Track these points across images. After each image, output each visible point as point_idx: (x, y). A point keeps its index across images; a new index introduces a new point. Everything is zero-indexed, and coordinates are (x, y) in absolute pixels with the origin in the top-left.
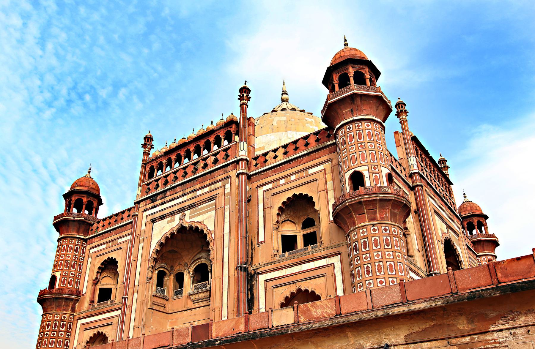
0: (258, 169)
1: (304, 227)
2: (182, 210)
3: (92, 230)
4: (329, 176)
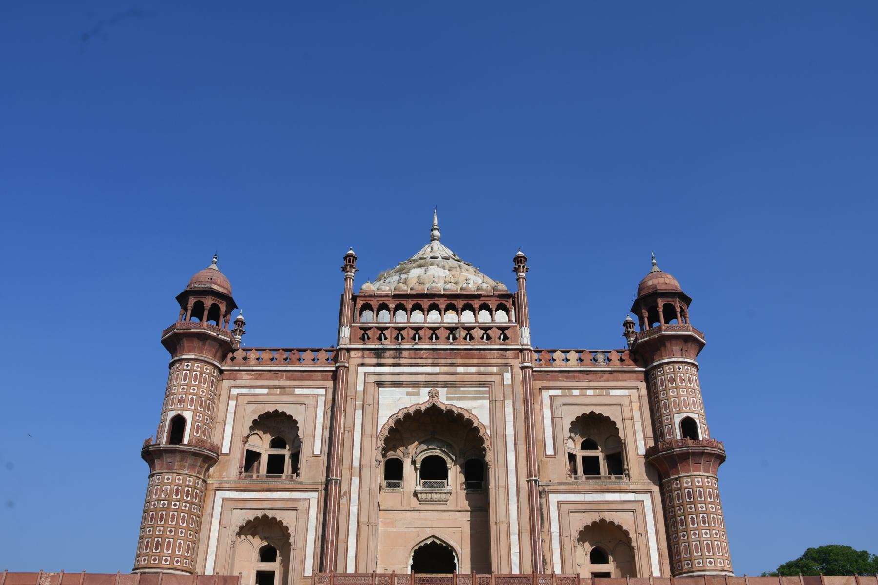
0: (541, 366)
1: (585, 446)
2: (435, 384)
3: (233, 359)
4: (636, 406)
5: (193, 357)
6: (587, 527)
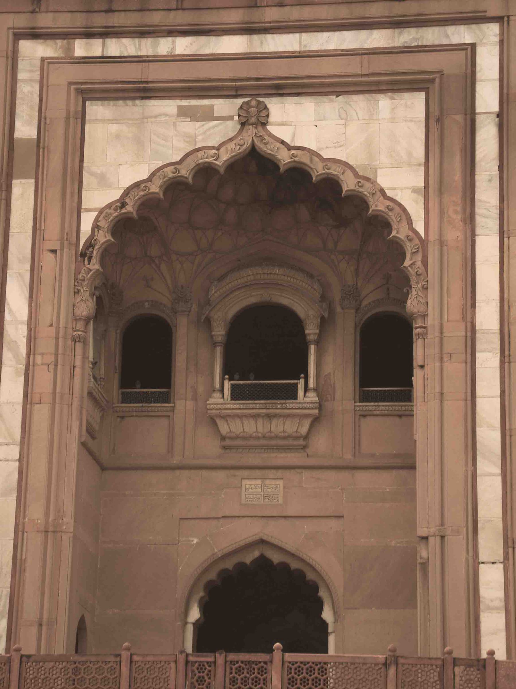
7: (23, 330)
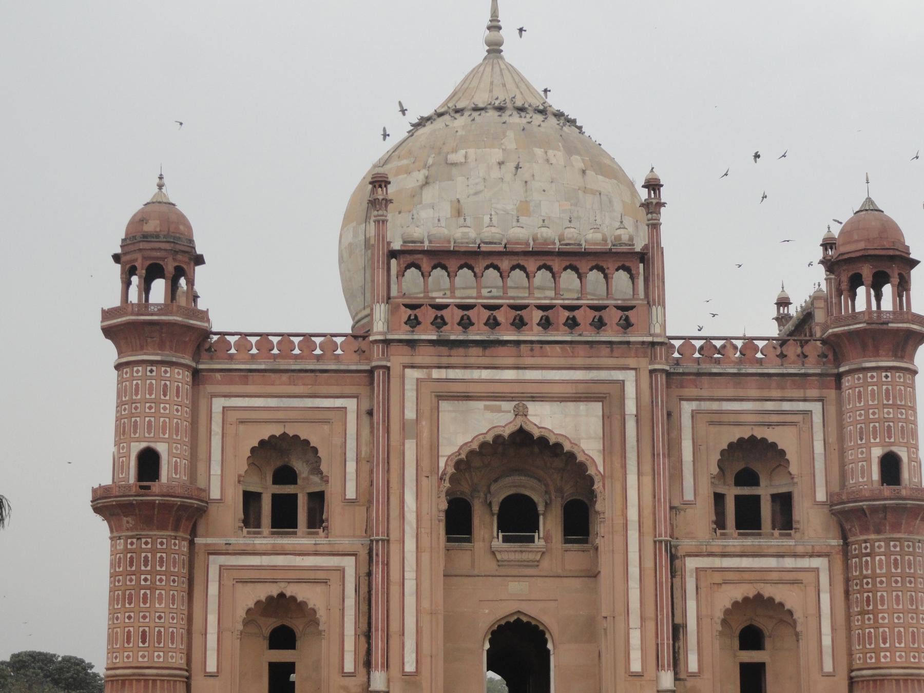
5: (158, 358)
6: (736, 604)
7: (414, 515)
